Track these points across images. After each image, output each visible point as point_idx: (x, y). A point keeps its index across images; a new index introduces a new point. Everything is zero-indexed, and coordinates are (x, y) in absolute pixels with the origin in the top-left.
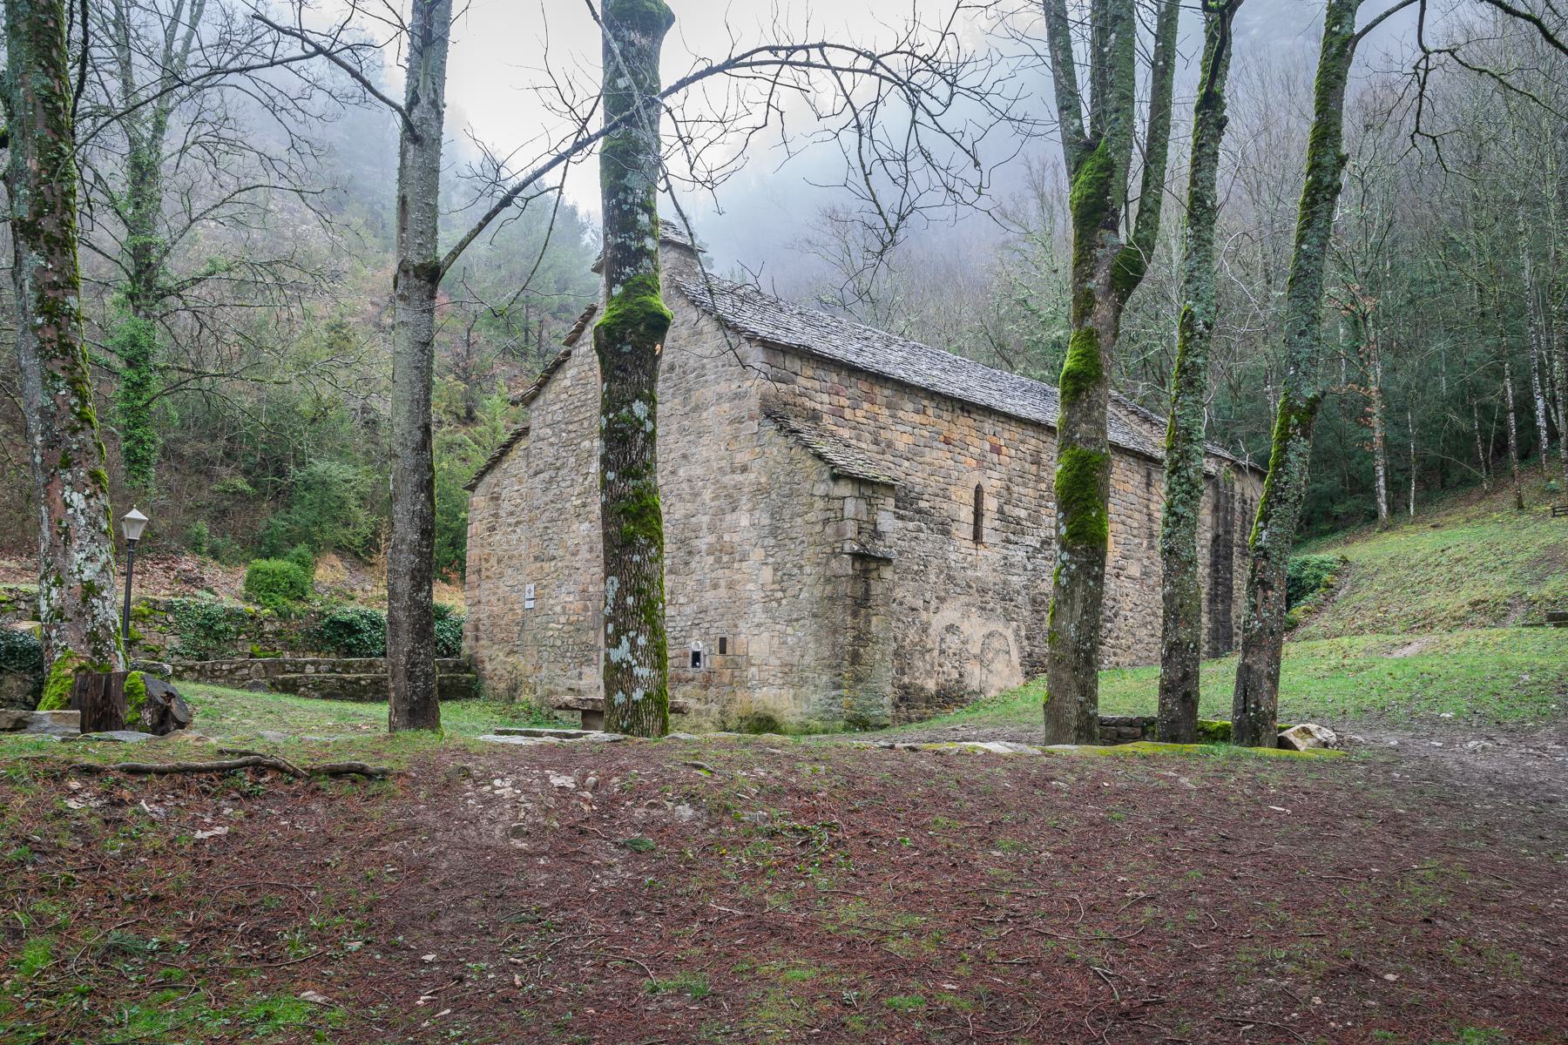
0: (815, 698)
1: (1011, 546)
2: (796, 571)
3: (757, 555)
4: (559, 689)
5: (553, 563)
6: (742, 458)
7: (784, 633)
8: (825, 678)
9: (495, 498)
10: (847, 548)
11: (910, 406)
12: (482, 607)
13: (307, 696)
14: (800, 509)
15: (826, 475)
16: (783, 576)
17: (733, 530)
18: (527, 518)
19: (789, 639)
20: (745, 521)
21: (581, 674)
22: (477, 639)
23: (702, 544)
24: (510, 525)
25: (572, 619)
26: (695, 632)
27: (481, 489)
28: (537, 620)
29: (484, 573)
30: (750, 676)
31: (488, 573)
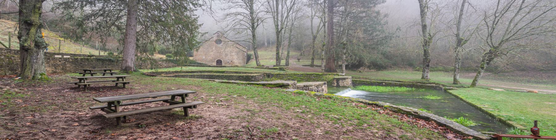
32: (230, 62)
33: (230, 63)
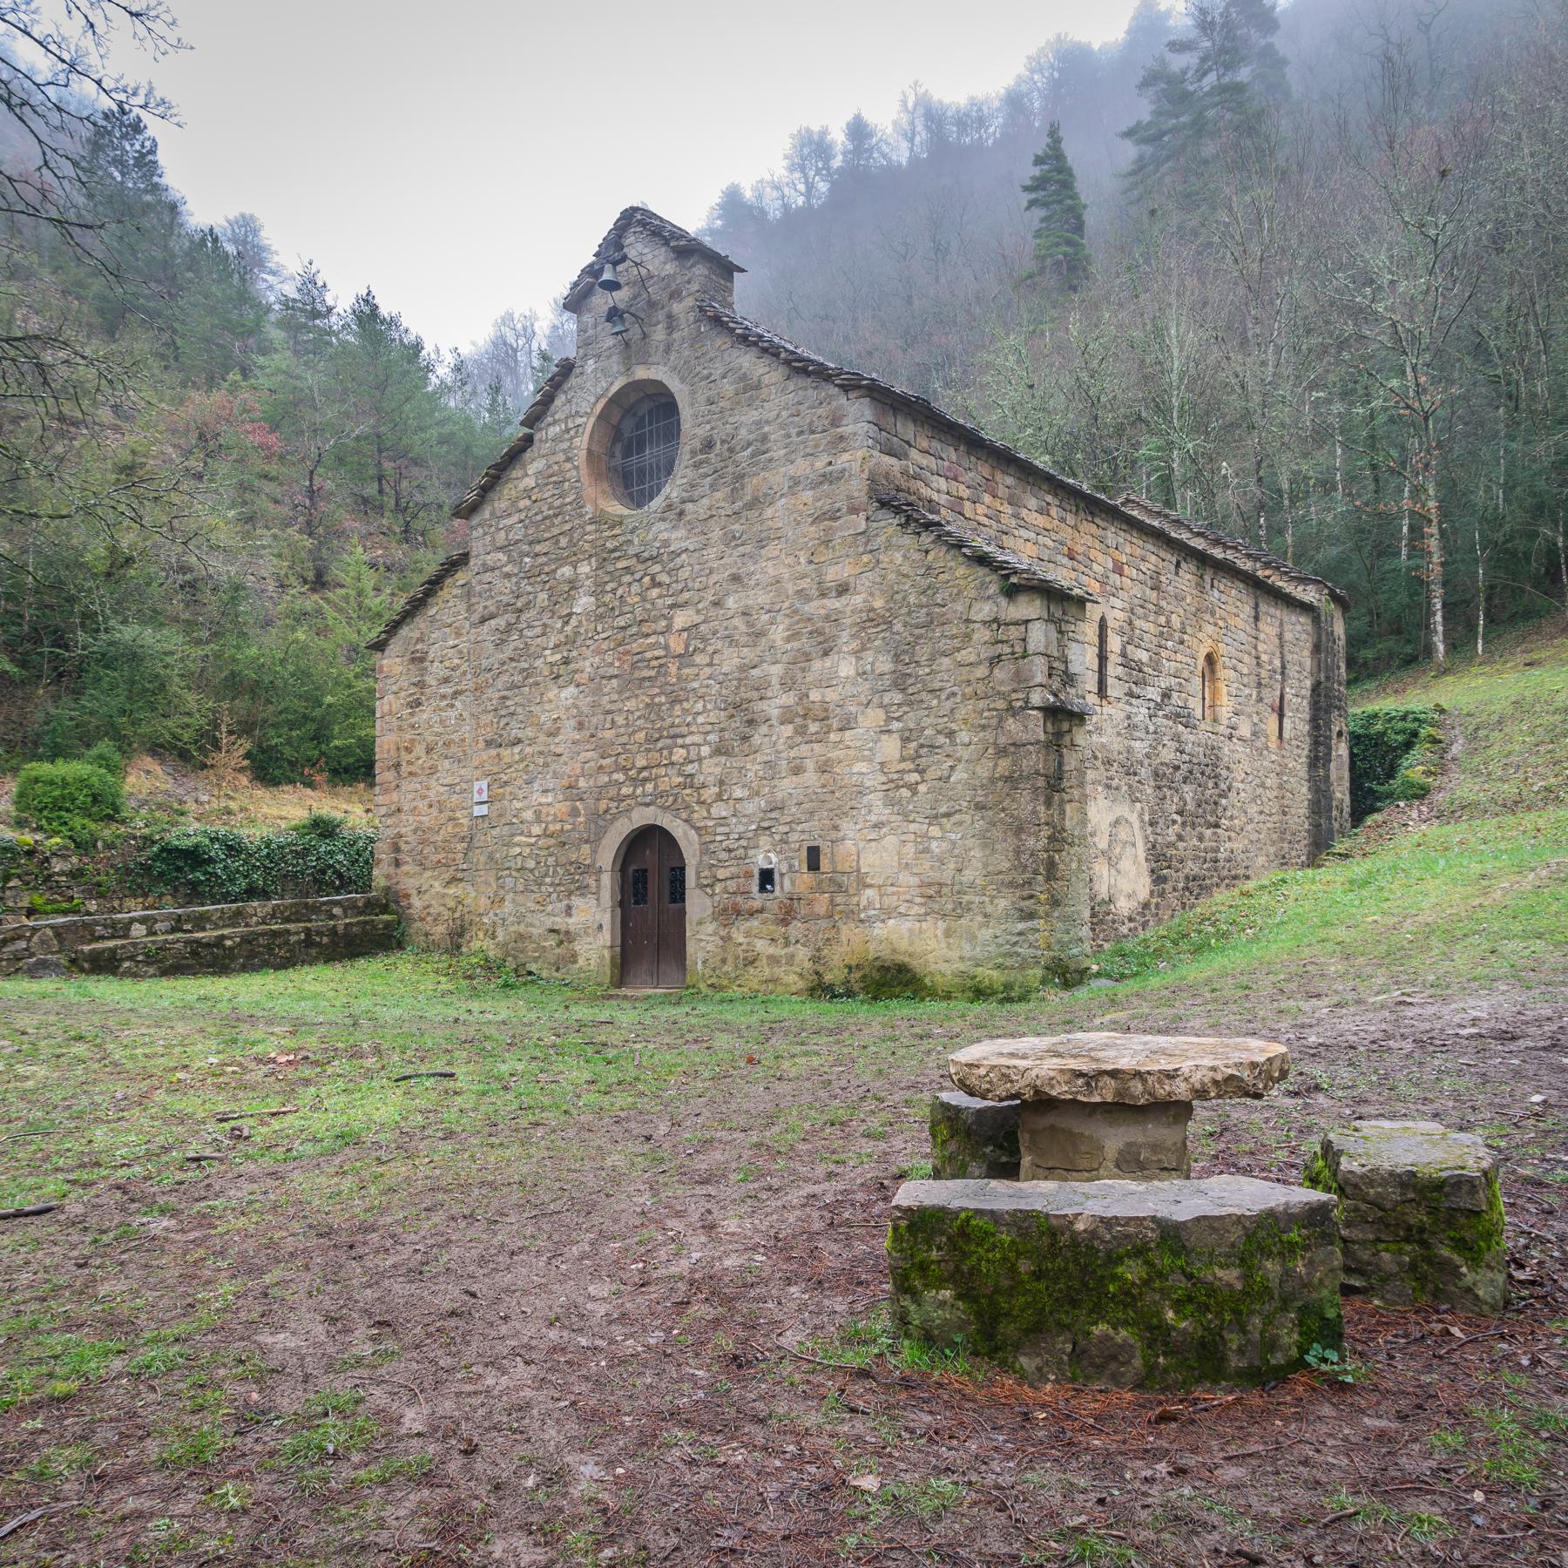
0: (985, 934)
1: (1134, 701)
2: (942, 740)
3: (872, 718)
4: (535, 931)
5: (517, 749)
6: (834, 574)
7: (925, 836)
8: (1002, 903)
9: (418, 659)
10: (1036, 698)
11: (1033, 503)
12: (403, 817)
13: (135, 975)
14: (943, 645)
15: (993, 589)
16: (918, 750)
17: (827, 683)
18: (471, 685)
19: (934, 845)
20: (847, 669)
21: (569, 908)
22: (397, 864)
23: (775, 704)
24: (444, 697)
25: (552, 828)
26: (764, 841)
27: (395, 646)
28: (494, 832)
29: (405, 769)
30: (864, 902)
31: (412, 769)
33: (787, 916)
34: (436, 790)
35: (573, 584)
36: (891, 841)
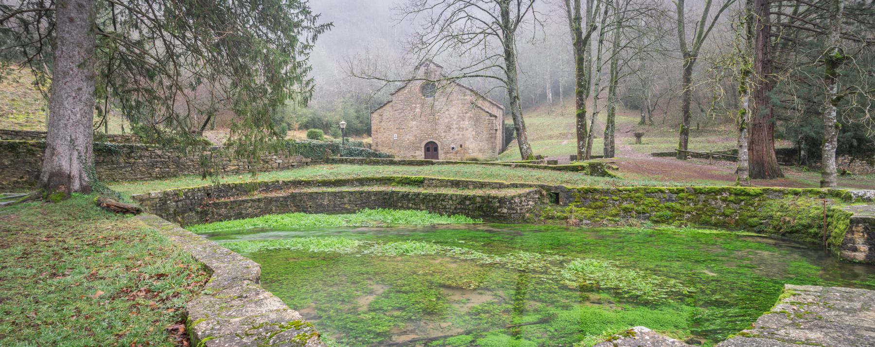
3: (471, 129)
16: (478, 134)
23: (455, 126)
26: (453, 144)
32: (457, 148)
33: (457, 153)
34: (385, 135)
35: (416, 107)
36: (474, 144)
